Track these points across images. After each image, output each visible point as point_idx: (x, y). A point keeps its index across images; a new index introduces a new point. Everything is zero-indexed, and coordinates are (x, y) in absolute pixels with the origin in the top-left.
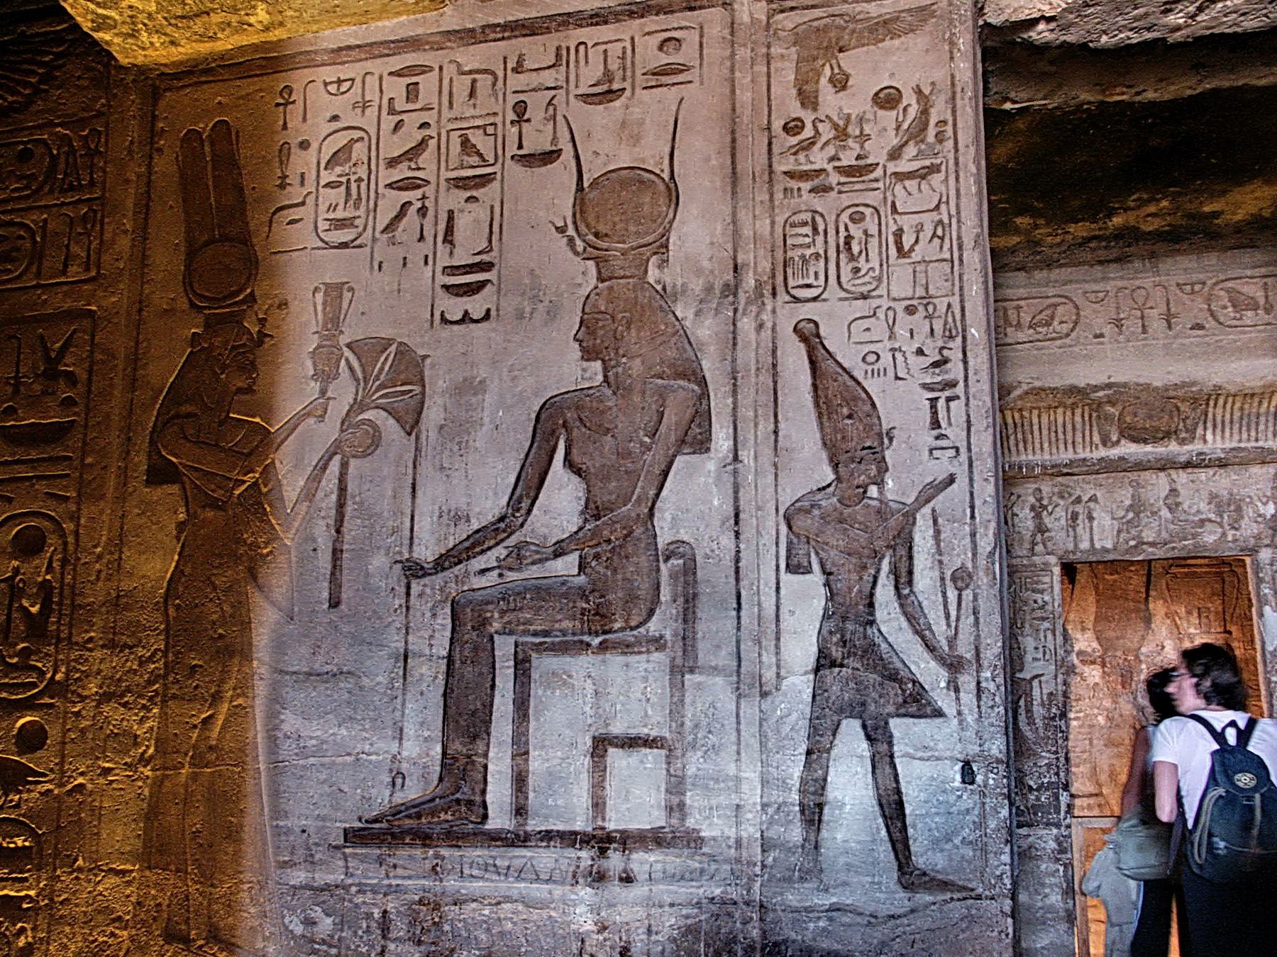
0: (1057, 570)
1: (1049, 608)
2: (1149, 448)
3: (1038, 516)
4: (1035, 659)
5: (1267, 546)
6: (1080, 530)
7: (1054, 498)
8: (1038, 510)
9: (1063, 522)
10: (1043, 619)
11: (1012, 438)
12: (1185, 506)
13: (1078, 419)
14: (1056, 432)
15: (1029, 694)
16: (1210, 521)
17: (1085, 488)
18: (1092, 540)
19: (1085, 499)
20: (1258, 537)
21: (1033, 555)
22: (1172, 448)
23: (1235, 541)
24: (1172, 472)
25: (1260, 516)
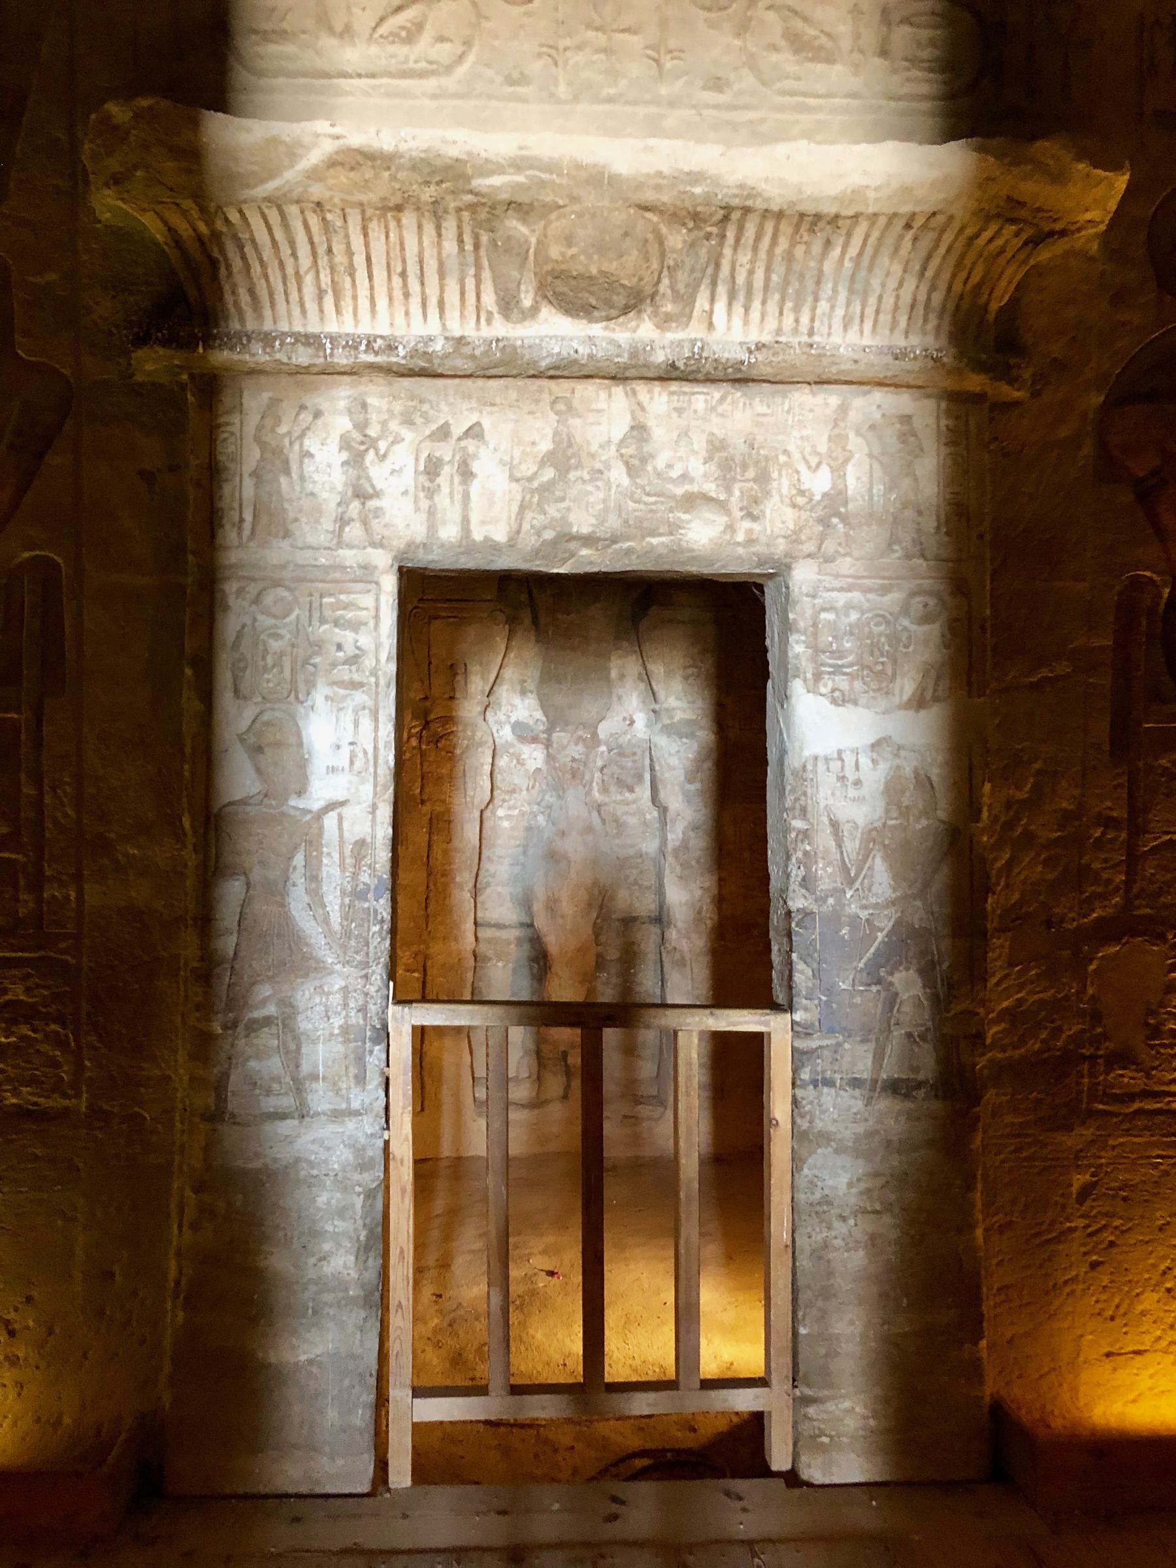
0: (389, 584)
1: (368, 662)
2: (597, 329)
3: (356, 460)
4: (333, 770)
5: (809, 556)
6: (442, 500)
7: (394, 425)
8: (357, 451)
9: (408, 479)
10: (355, 685)
11: (309, 279)
12: (660, 462)
13: (450, 246)
14: (403, 275)
15: (313, 842)
16: (707, 499)
17: (455, 407)
18: (465, 522)
19: (457, 430)
20: (794, 538)
21: (340, 545)
22: (643, 334)
23: (750, 542)
24: (641, 388)
25: (802, 493)
